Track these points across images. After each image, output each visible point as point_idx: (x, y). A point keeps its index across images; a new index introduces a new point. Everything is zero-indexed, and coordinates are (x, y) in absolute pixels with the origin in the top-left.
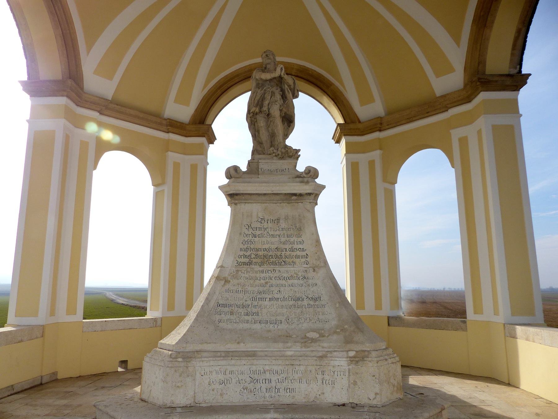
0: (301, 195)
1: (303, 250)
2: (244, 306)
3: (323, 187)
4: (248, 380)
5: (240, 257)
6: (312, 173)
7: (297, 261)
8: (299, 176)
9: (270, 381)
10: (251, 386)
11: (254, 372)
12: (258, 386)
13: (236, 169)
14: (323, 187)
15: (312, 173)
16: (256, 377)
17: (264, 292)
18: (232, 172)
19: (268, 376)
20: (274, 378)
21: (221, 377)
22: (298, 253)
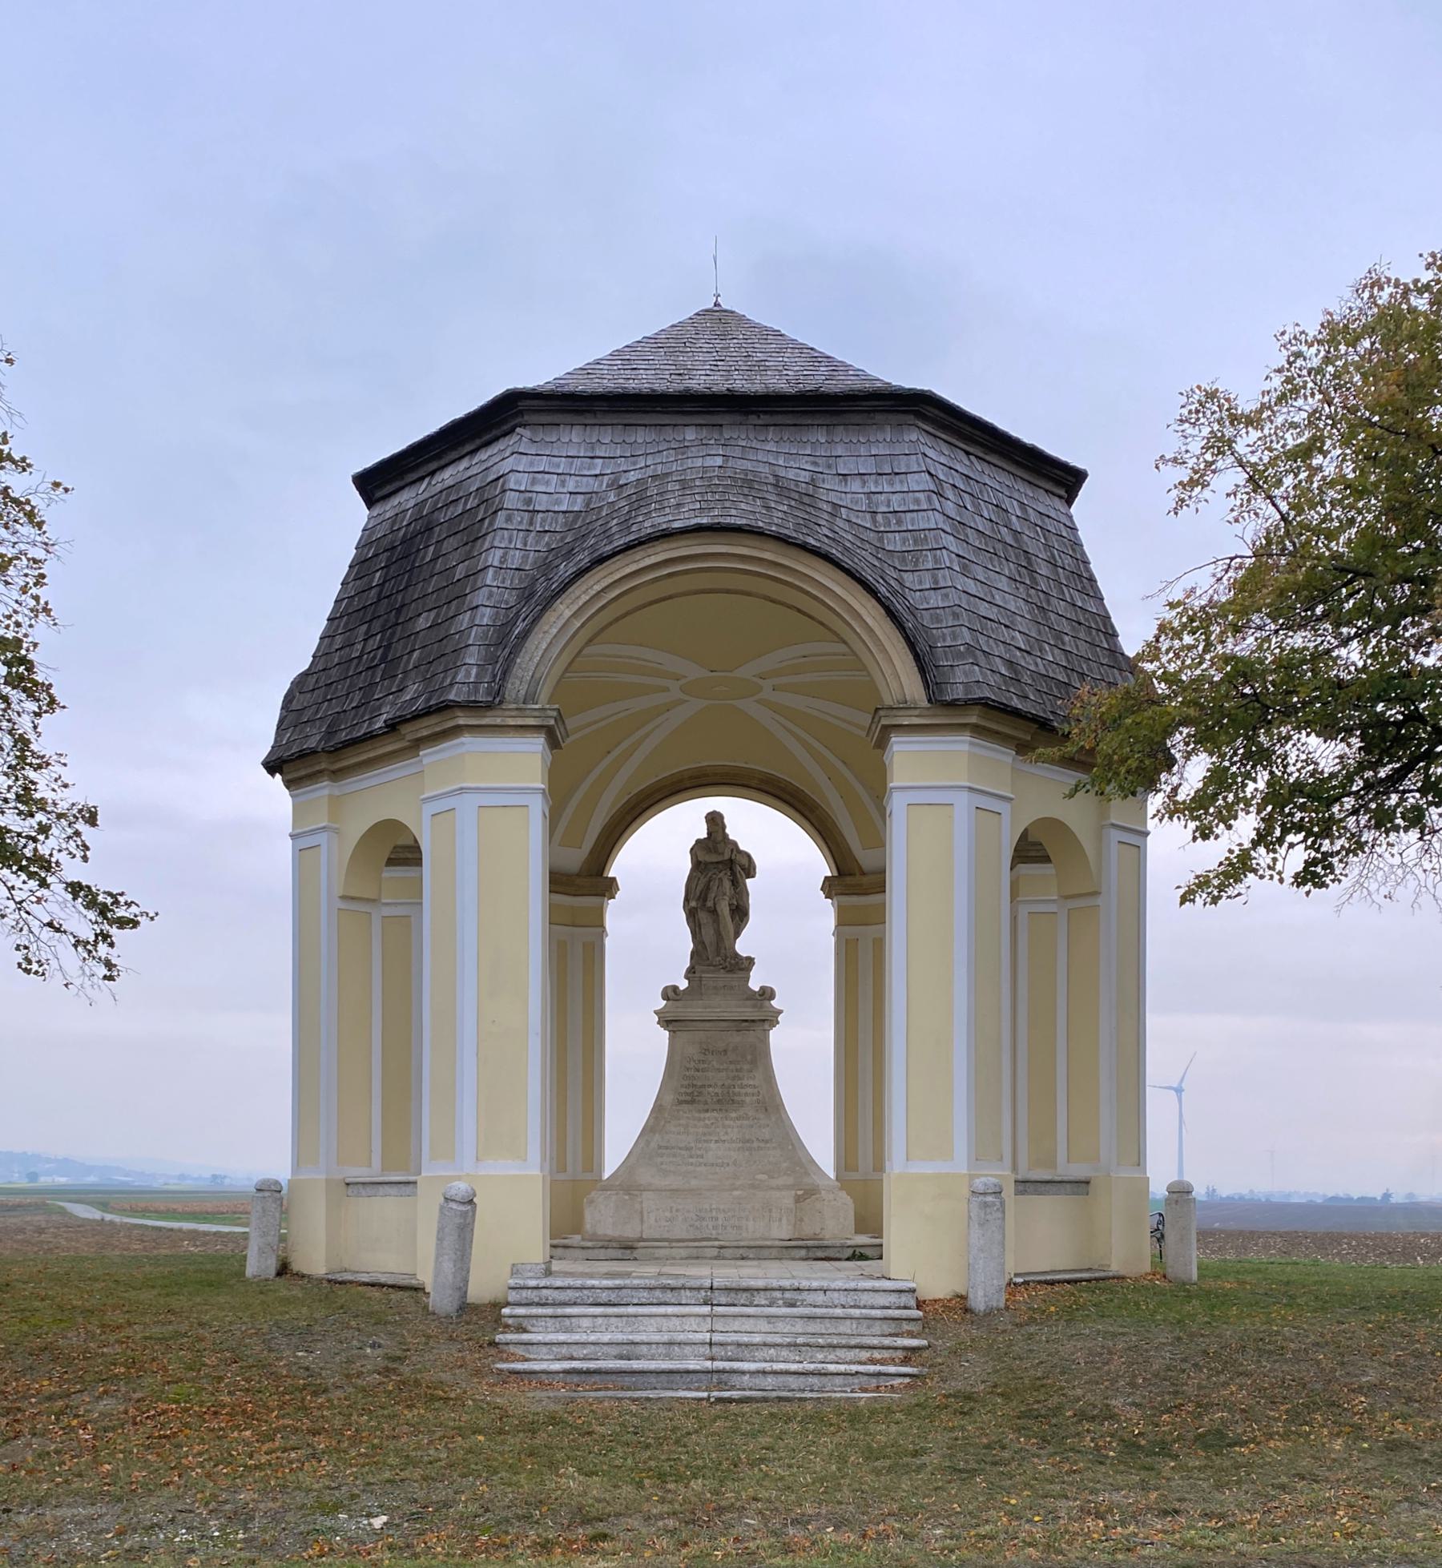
0: (753, 1021)
1: (755, 1087)
2: (687, 1149)
3: (780, 1012)
4: (695, 1218)
5: (680, 1094)
6: (767, 994)
7: (748, 1099)
8: (751, 996)
9: (717, 1219)
10: (697, 1223)
11: (700, 1211)
12: (704, 1223)
13: (675, 988)
14: (780, 1012)
15: (767, 994)
16: (702, 1214)
17: (710, 1134)
18: (671, 994)
19: (714, 1214)
20: (721, 1216)
21: (668, 1214)
22: (749, 1090)
